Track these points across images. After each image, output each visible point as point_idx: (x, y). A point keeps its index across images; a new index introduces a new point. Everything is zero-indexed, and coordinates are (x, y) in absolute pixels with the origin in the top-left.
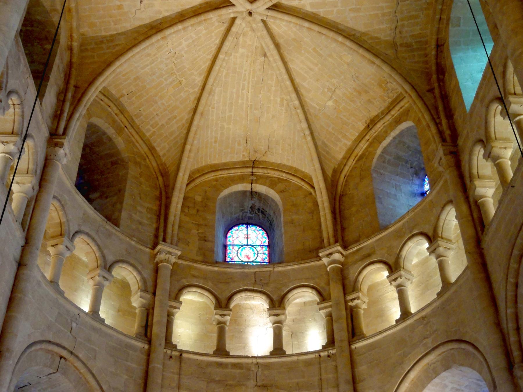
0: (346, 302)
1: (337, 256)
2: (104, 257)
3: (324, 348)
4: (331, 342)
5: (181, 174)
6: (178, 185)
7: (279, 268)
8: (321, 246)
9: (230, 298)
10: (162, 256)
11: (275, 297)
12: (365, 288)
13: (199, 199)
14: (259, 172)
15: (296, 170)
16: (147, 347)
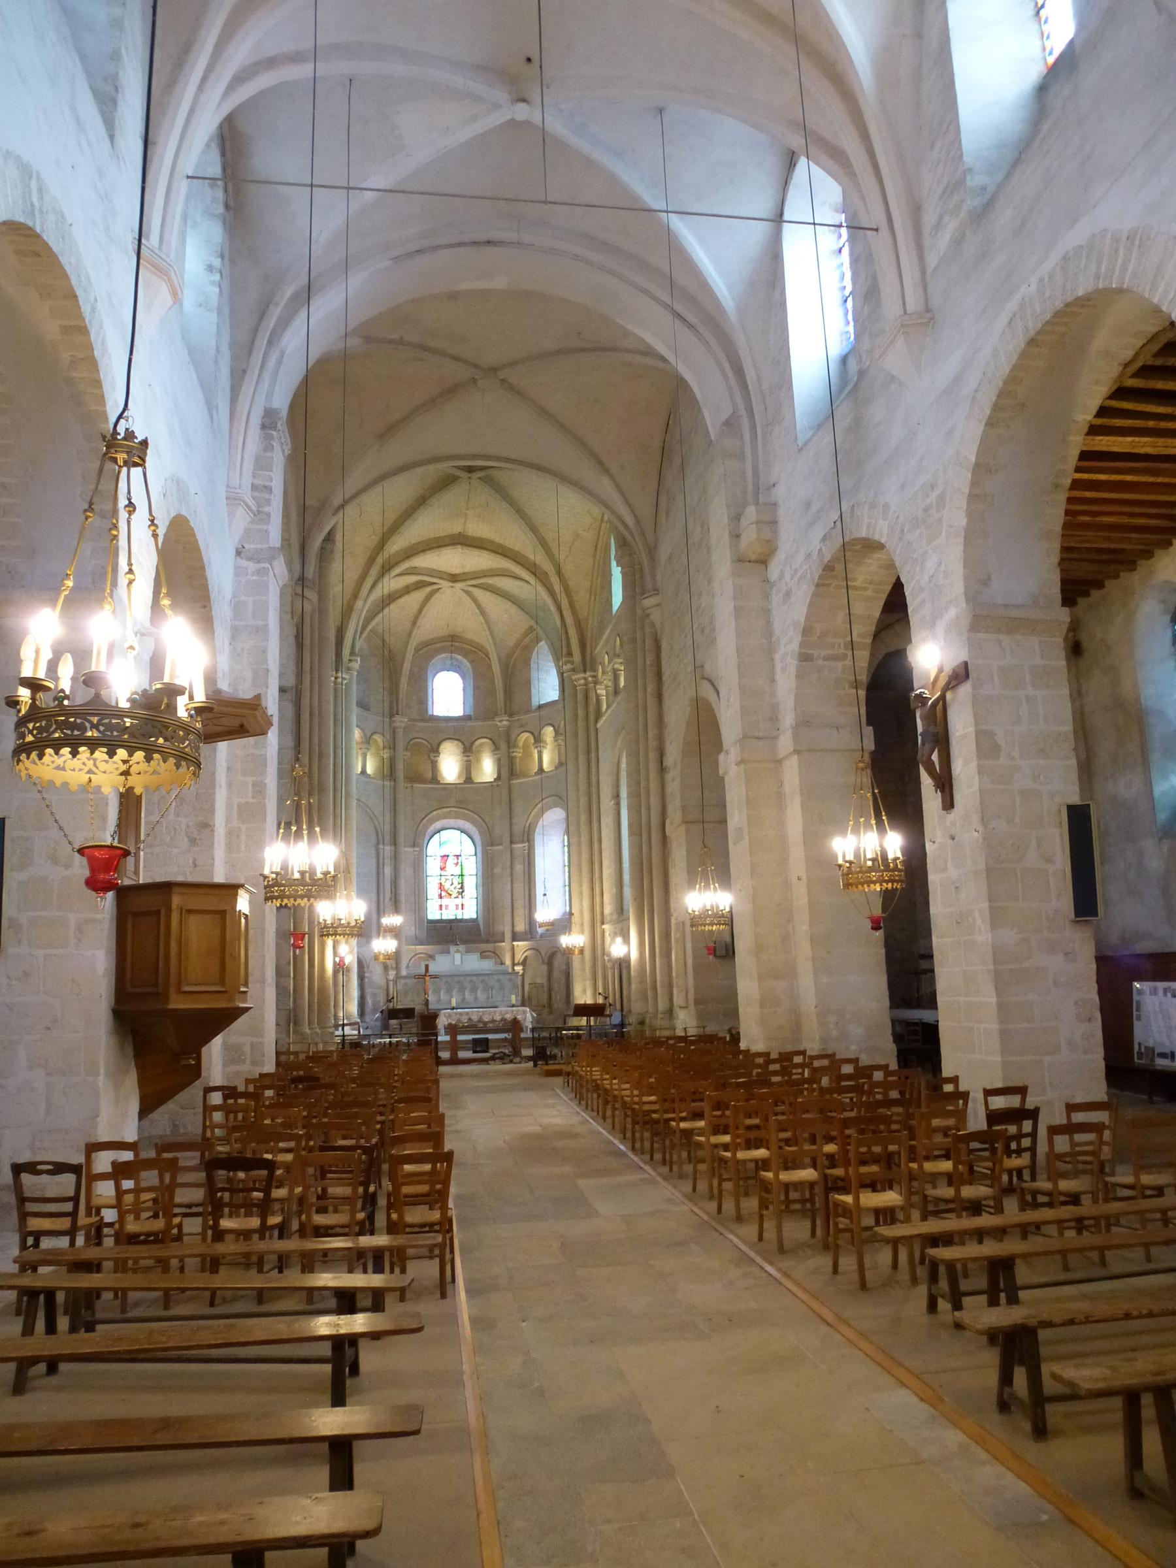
0: (509, 753)
1: (505, 723)
2: (365, 735)
3: (495, 780)
4: (499, 778)
5: (405, 665)
6: (404, 673)
7: (470, 724)
8: (496, 714)
9: (439, 745)
10: (394, 725)
11: (467, 744)
12: (521, 744)
13: (416, 670)
14: (457, 644)
15: (483, 647)
16: (393, 783)
